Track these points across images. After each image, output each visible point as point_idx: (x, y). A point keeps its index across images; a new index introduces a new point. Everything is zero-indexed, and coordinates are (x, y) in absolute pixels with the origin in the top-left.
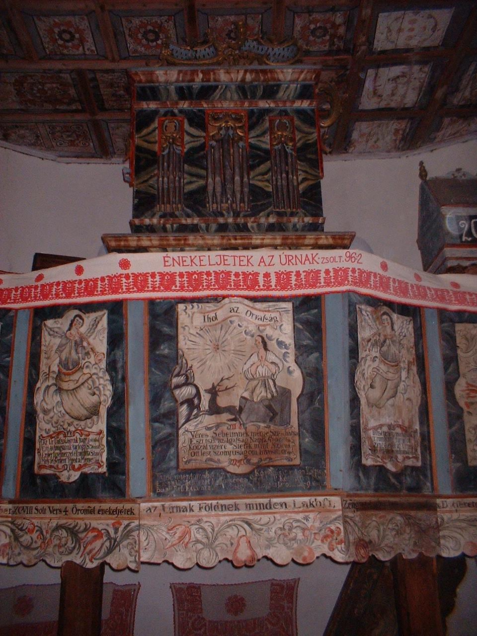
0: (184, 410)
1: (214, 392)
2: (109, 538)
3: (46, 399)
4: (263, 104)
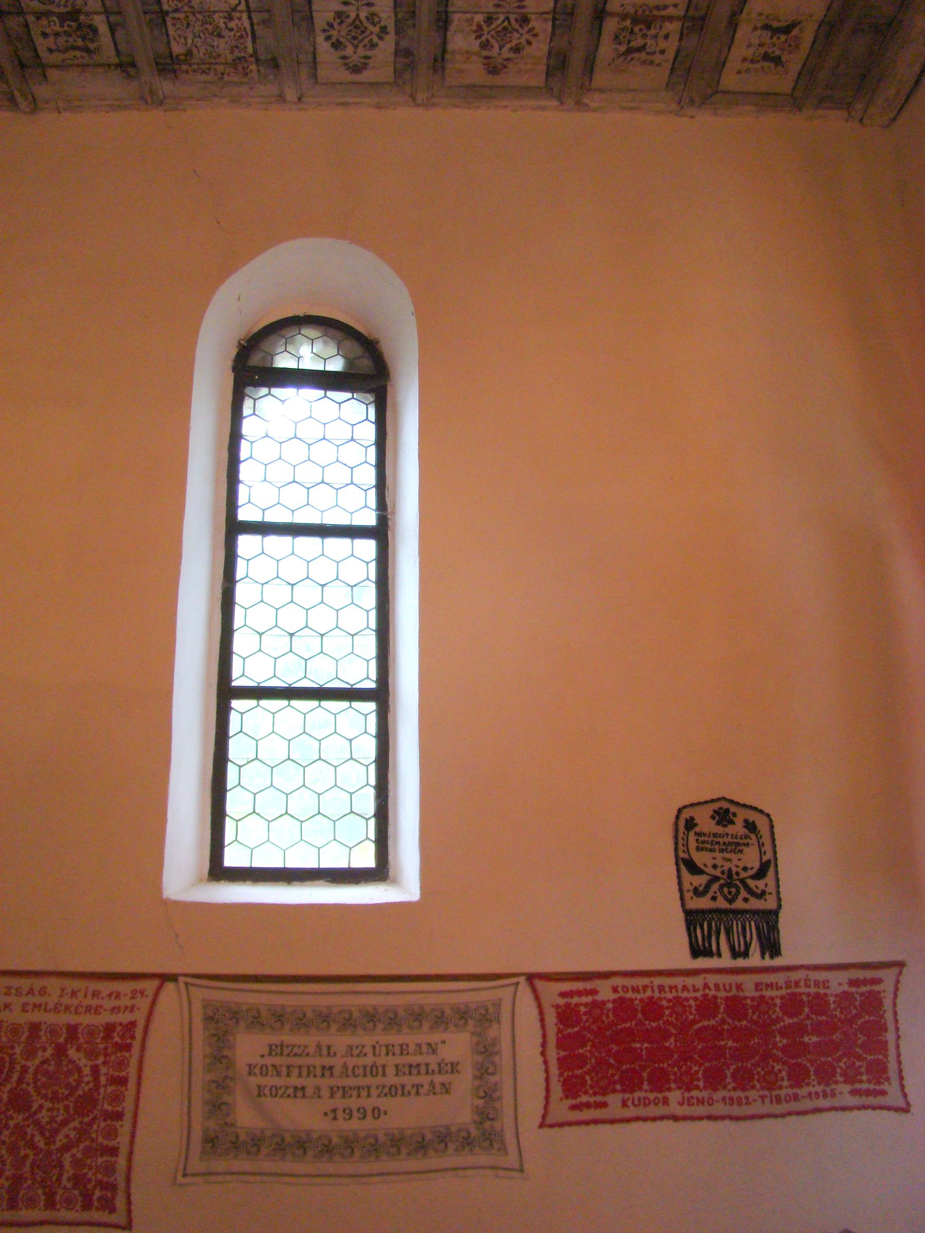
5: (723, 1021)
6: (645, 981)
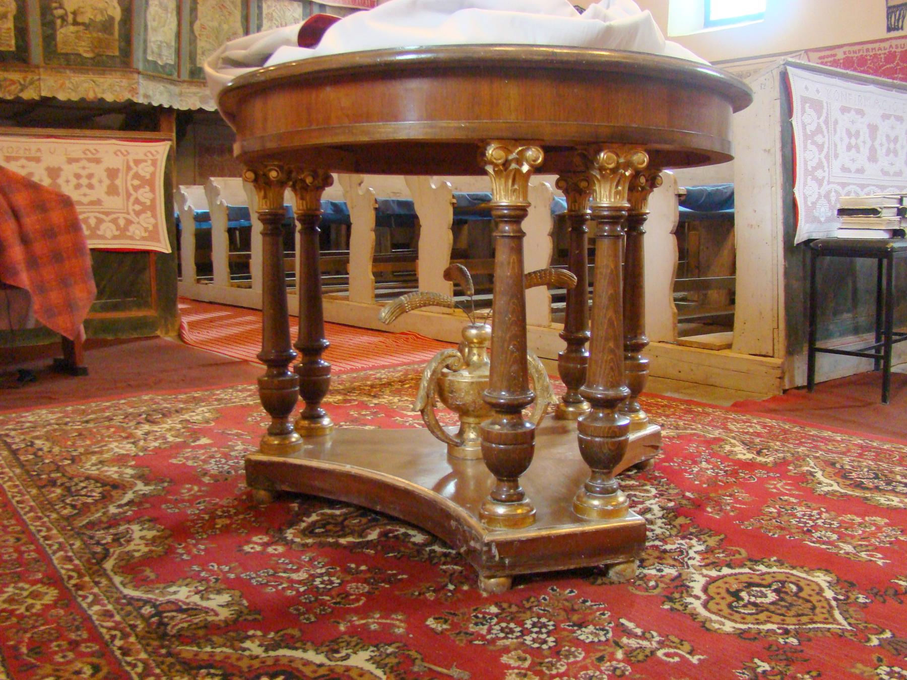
0: (59, 22)
1: (75, 14)
2: (21, 84)
5: (898, 64)
6: (860, 47)
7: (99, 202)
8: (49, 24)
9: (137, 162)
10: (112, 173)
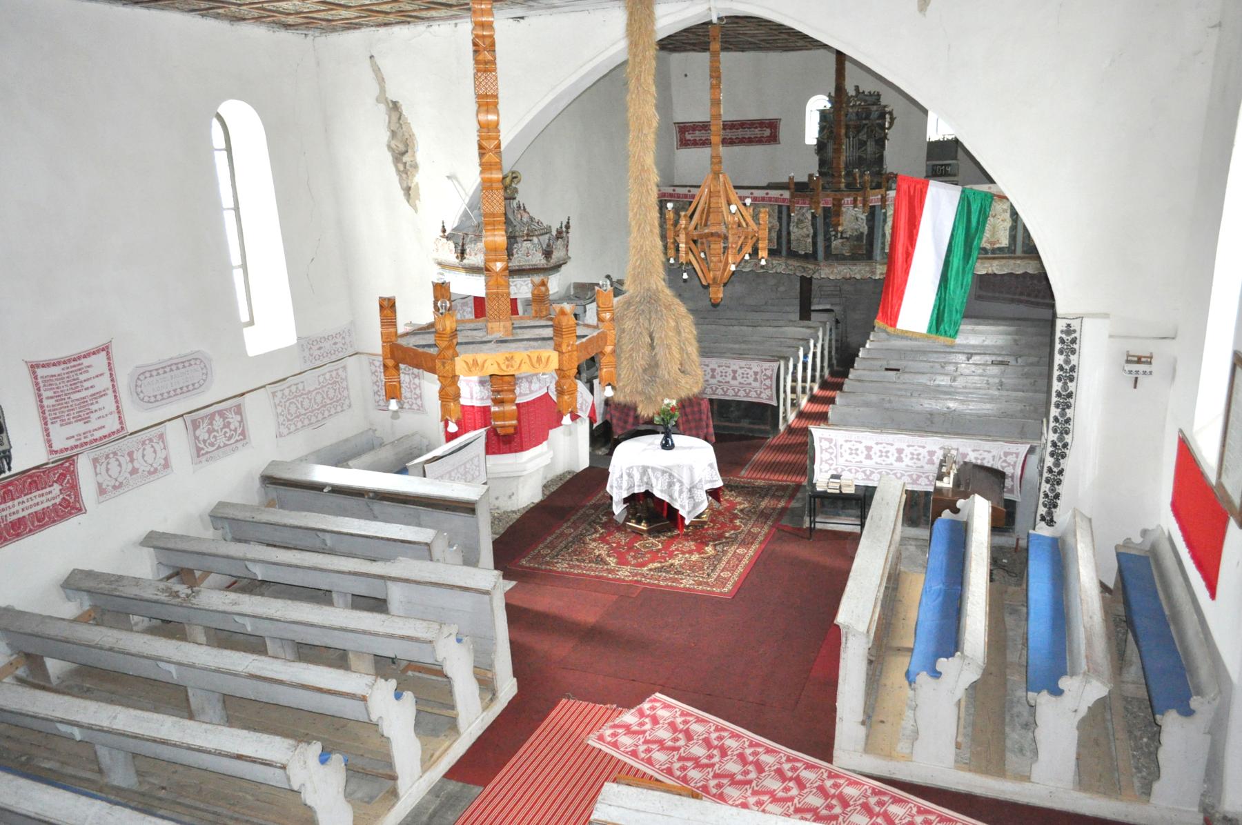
0: (833, 238)
3: (793, 229)
4: (864, 122)
7: (750, 384)
8: (828, 240)
9: (766, 370)
10: (756, 373)
